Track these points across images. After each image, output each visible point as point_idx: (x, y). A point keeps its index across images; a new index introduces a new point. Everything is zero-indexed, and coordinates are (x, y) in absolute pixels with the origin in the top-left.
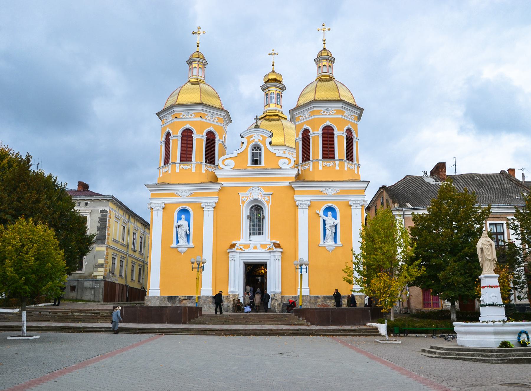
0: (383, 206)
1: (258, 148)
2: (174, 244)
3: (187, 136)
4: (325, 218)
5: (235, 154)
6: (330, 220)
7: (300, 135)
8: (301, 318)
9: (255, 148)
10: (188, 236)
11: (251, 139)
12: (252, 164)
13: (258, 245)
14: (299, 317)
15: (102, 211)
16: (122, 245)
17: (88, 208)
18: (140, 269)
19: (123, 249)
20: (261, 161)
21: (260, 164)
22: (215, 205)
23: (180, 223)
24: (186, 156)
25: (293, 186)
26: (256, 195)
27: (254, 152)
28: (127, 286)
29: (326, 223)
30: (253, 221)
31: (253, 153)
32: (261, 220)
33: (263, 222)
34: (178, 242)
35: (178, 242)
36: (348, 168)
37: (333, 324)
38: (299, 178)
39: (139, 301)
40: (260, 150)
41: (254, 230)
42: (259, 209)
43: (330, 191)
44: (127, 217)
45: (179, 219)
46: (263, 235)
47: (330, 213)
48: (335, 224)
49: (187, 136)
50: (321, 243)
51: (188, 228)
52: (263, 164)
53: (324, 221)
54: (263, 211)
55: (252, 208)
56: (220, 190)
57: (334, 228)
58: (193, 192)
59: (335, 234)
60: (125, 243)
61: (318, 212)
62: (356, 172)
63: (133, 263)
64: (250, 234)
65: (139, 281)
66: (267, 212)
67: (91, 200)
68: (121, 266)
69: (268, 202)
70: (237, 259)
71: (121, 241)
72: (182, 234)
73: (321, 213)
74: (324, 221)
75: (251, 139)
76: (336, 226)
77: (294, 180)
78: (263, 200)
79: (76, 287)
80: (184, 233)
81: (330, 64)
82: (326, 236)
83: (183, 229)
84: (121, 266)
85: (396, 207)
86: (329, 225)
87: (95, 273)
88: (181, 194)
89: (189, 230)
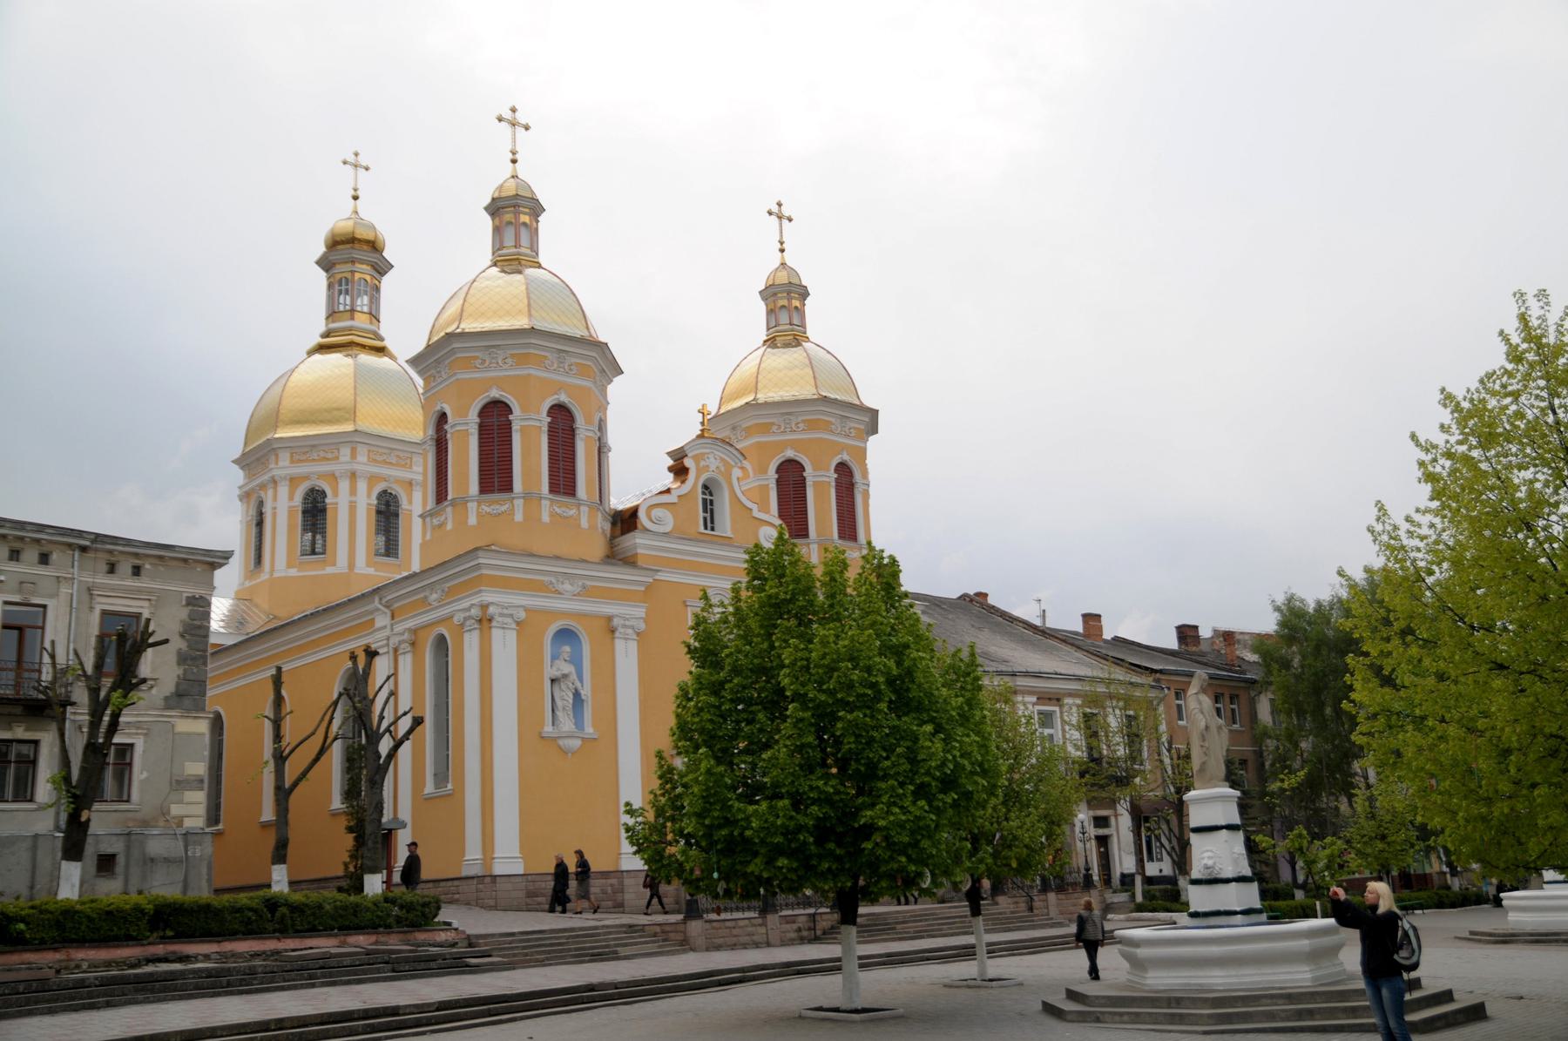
2: (548, 729)
5: (672, 498)
11: (702, 463)
17: (142, 583)
22: (642, 626)
45: (554, 658)
56: (649, 587)
58: (589, 583)
72: (565, 698)
75: (702, 463)
79: (121, 860)
87: (175, 810)
88: (560, 587)
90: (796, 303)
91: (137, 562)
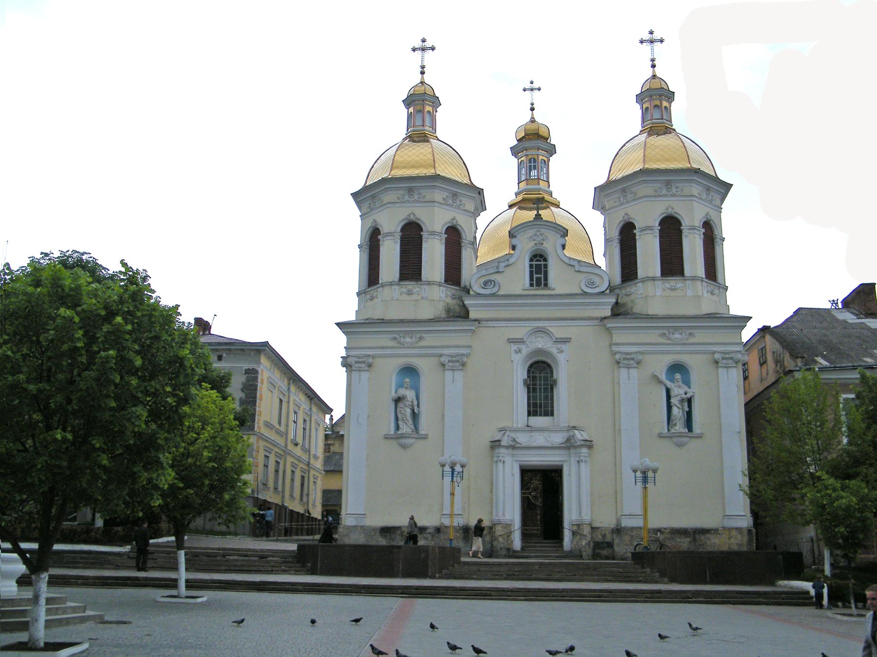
0: (765, 362)
1: (541, 256)
3: (412, 236)
4: (669, 384)
6: (678, 391)
7: (615, 234)
8: (648, 570)
9: (535, 256)
10: (415, 416)
12: (532, 285)
14: (643, 567)
15: (248, 372)
16: (278, 432)
18: (303, 477)
19: (280, 441)
20: (546, 279)
21: (546, 285)
23: (402, 392)
24: (411, 268)
25: (609, 325)
26: (541, 343)
27: (534, 263)
28: (286, 508)
29: (672, 394)
31: (531, 266)
32: (551, 386)
33: (552, 392)
34: (397, 428)
35: (397, 428)
37: (712, 582)
38: (619, 311)
39: (302, 535)
40: (545, 260)
42: (544, 368)
43: (677, 336)
44: (286, 382)
45: (400, 386)
46: (552, 415)
47: (678, 376)
48: (689, 395)
49: (412, 236)
51: (415, 403)
53: (668, 391)
55: (531, 366)
57: (686, 404)
59: (689, 414)
60: (283, 429)
63: (294, 465)
64: (529, 414)
65: (301, 499)
67: (230, 350)
68: (277, 471)
70: (508, 460)
71: (277, 426)
73: (663, 377)
74: (668, 391)
76: (689, 401)
77: (608, 313)
78: (554, 351)
80: (408, 411)
81: (665, 104)
82: (673, 417)
83: (407, 403)
84: (277, 471)
85: (799, 364)
86: (679, 398)
89: (418, 406)
90: (665, 104)
91: (219, 353)
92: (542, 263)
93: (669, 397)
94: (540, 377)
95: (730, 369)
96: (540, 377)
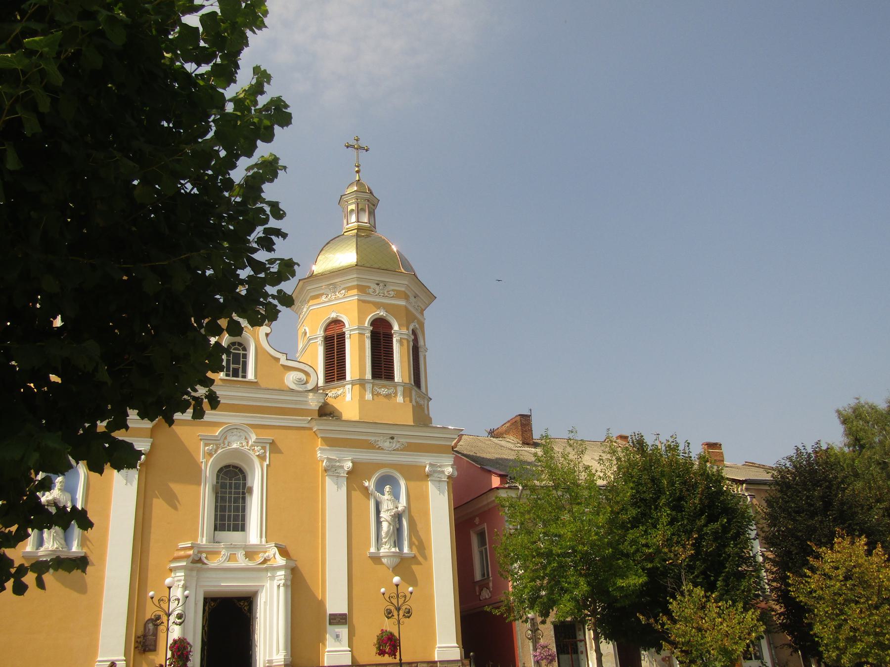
13: (240, 555)
21: (244, 377)
30: (223, 499)
36: (417, 402)
40: (245, 349)
41: (223, 518)
42: (236, 474)
50: (373, 549)
52: (251, 375)
54: (245, 478)
59: (399, 531)
61: (367, 484)
62: (426, 412)
64: (215, 529)
66: (256, 481)
69: (262, 458)
82: (383, 534)
86: (389, 514)
92: (241, 352)
93: (378, 512)
94: (230, 484)
95: (442, 483)
96: (230, 484)
